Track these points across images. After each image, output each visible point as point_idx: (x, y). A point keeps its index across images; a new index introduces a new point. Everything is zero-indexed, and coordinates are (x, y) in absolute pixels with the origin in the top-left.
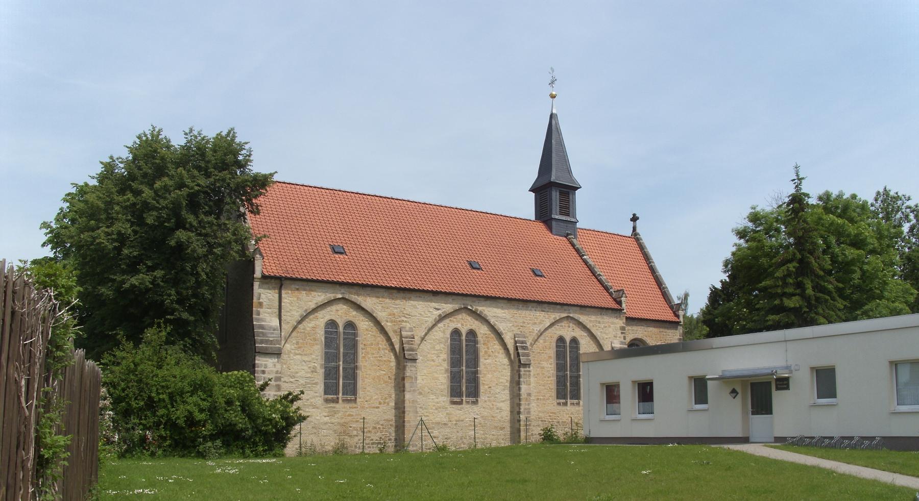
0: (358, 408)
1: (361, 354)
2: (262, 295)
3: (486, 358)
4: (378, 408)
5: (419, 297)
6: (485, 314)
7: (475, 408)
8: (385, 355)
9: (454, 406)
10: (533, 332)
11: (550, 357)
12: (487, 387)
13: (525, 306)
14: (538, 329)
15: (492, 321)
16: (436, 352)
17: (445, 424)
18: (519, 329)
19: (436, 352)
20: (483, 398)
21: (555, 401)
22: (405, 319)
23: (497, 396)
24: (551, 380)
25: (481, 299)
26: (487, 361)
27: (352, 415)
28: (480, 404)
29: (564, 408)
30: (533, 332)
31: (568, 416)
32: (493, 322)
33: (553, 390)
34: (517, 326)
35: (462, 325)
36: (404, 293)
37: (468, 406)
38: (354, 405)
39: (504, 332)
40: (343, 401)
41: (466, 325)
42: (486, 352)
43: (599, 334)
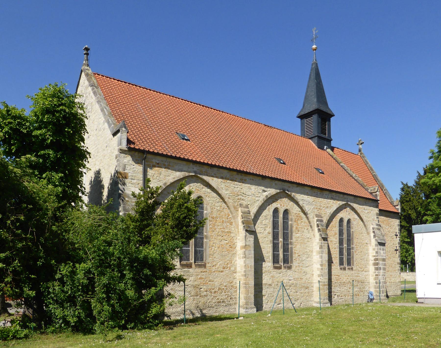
0: (207, 272)
1: (209, 225)
2: (127, 166)
3: (297, 232)
4: (222, 272)
5: (253, 180)
6: (297, 198)
7: (289, 272)
8: (227, 227)
9: (275, 270)
10: (326, 214)
11: (336, 234)
12: (297, 255)
13: (322, 193)
14: (329, 212)
15: (301, 203)
16: (263, 226)
17: (270, 285)
18: (318, 211)
19: (263, 226)
20: (295, 264)
21: (339, 267)
22: (243, 198)
23: (303, 262)
24: (336, 251)
25: (294, 185)
26: (297, 235)
27: (202, 278)
28: (293, 268)
29: (344, 272)
30: (326, 214)
31: (346, 278)
32: (302, 204)
33: (337, 259)
34: (317, 208)
35: (281, 205)
36: (241, 175)
37: (285, 270)
38: (205, 270)
39: (309, 212)
40: (196, 266)
41: (284, 206)
42: (297, 228)
43: (364, 217)
